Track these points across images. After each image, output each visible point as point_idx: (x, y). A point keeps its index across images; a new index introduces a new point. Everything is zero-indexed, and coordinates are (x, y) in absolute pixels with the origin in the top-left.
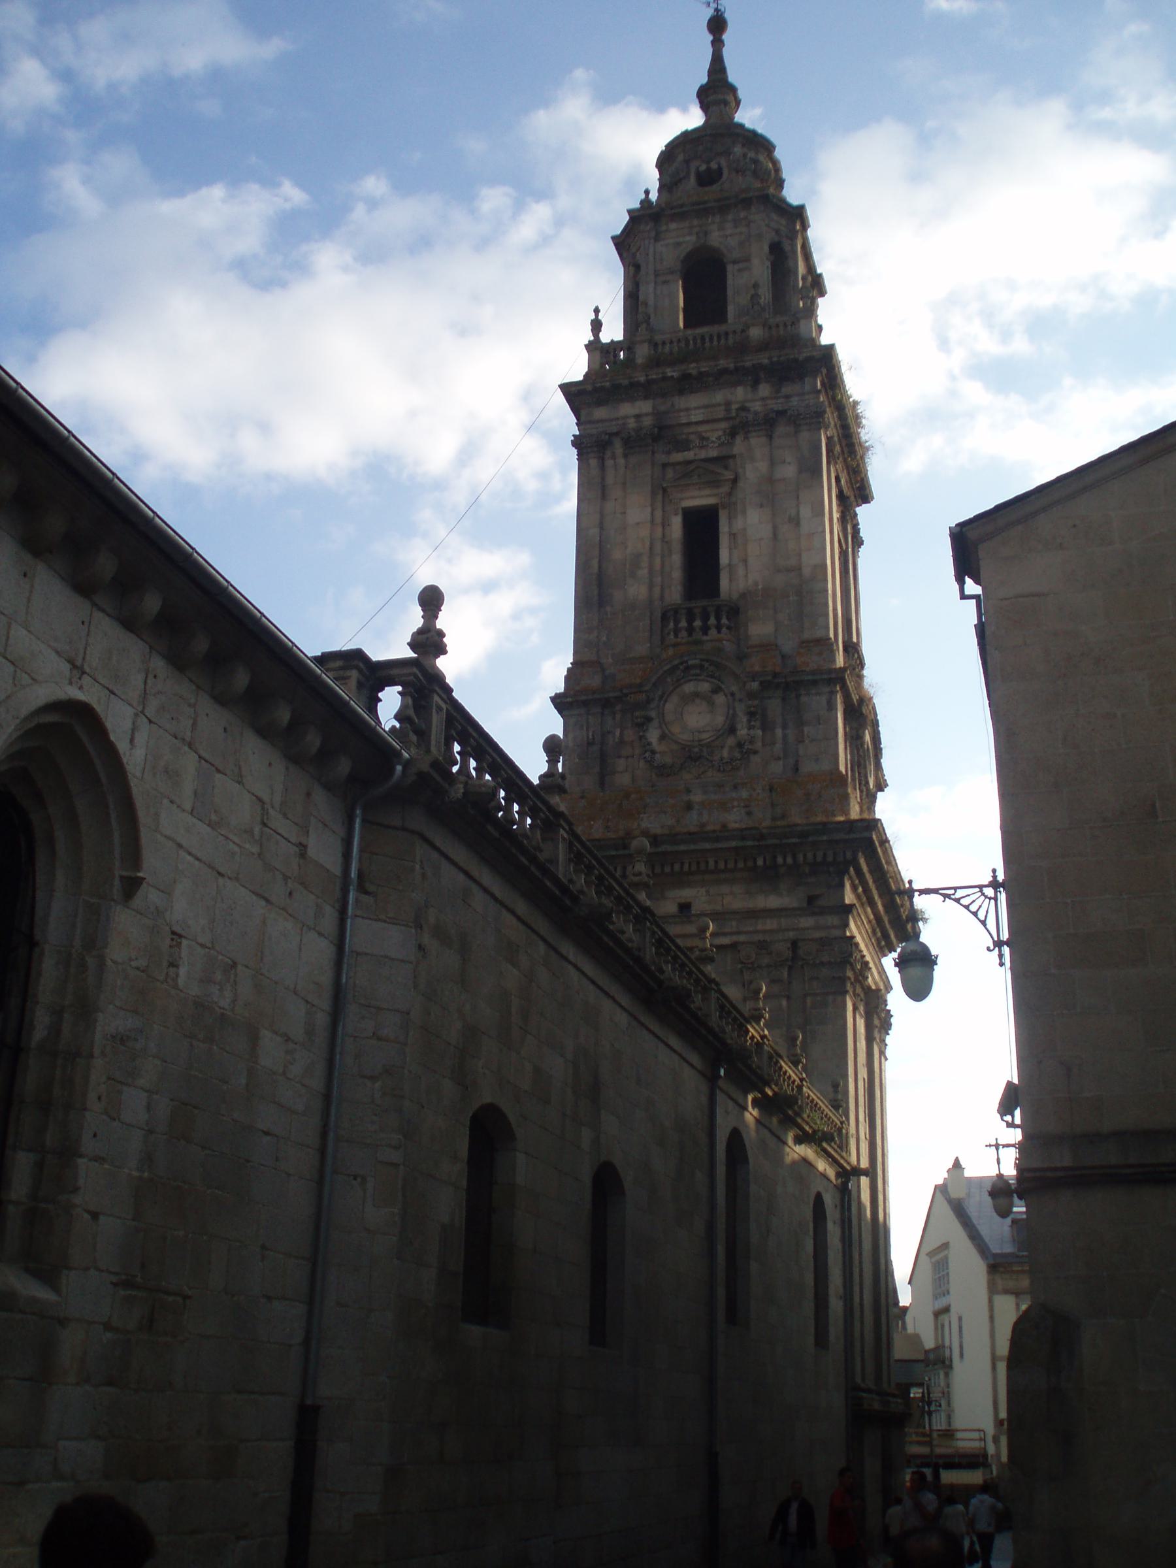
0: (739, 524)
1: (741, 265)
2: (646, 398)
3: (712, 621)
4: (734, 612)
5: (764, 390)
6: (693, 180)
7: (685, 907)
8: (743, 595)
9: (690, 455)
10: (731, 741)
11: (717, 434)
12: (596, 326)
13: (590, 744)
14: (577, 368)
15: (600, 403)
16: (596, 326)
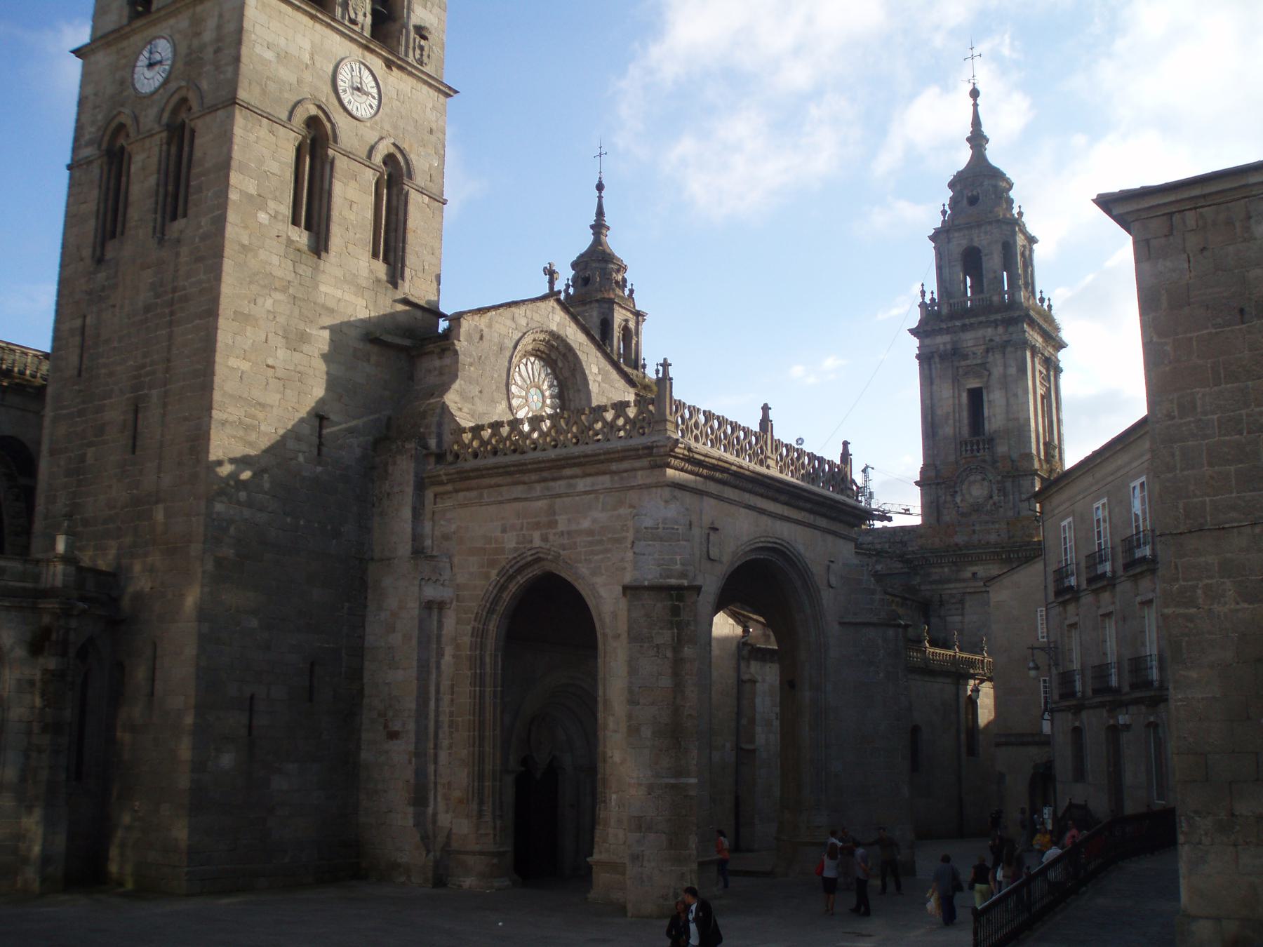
0: (992, 397)
2: (947, 334)
3: (981, 446)
4: (991, 440)
5: (1000, 330)
6: (965, 202)
7: (974, 574)
8: (995, 431)
9: (968, 362)
10: (991, 502)
11: (981, 351)
12: (923, 293)
13: (932, 503)
14: (914, 319)
15: (927, 336)
16: (923, 293)
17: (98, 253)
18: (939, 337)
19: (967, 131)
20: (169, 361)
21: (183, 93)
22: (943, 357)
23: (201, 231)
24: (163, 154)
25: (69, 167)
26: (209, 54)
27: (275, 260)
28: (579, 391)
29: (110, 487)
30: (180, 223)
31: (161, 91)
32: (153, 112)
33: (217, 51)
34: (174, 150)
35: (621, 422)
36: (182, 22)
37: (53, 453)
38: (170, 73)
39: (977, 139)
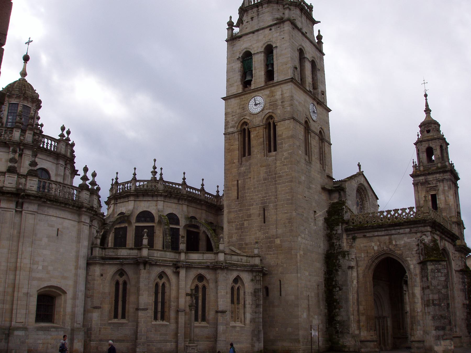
0: (439, 197)
1: (436, 150)
2: (423, 176)
6: (426, 132)
14: (411, 171)
16: (413, 162)
17: (240, 161)
18: (420, 177)
19: (424, 108)
20: (276, 195)
21: (271, 114)
22: (422, 184)
23: (284, 156)
24: (264, 132)
25: (224, 134)
26: (279, 102)
27: (303, 165)
28: (367, 201)
29: (256, 233)
30: (273, 153)
31: (261, 112)
32: (260, 119)
33: (282, 102)
34: (267, 130)
35: (412, 213)
36: (267, 92)
37: (229, 222)
38: (264, 107)
39: (428, 111)
